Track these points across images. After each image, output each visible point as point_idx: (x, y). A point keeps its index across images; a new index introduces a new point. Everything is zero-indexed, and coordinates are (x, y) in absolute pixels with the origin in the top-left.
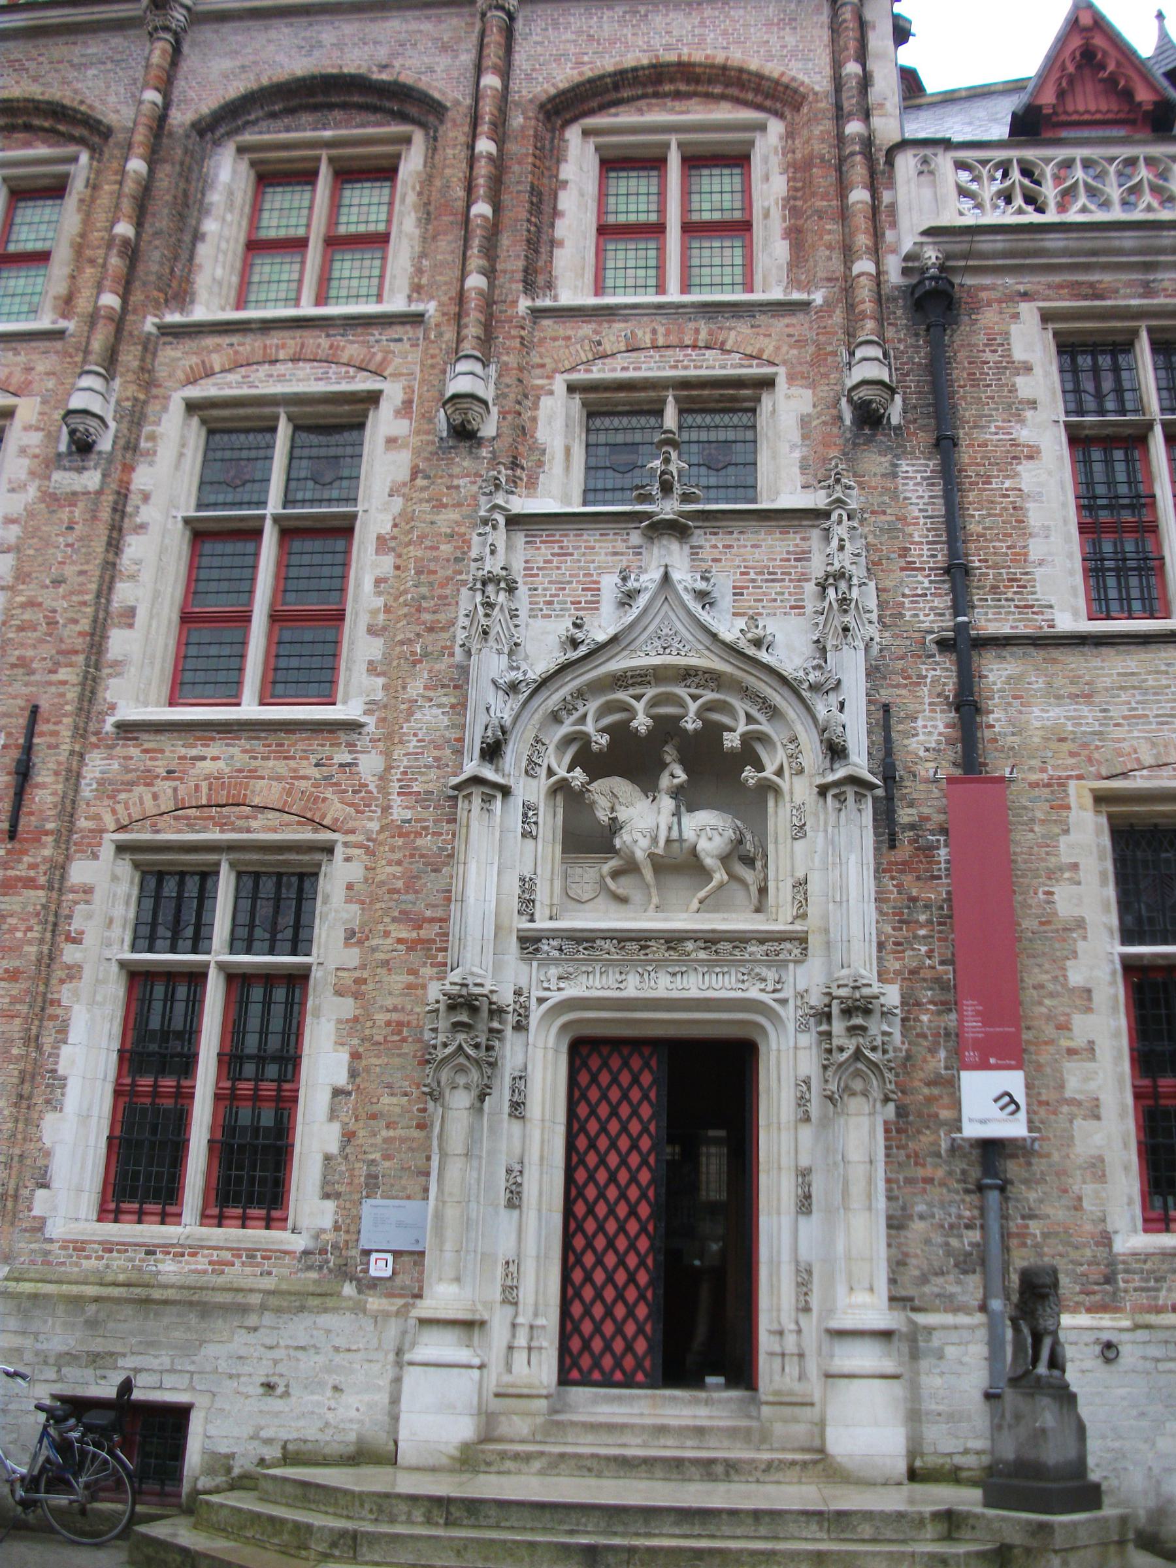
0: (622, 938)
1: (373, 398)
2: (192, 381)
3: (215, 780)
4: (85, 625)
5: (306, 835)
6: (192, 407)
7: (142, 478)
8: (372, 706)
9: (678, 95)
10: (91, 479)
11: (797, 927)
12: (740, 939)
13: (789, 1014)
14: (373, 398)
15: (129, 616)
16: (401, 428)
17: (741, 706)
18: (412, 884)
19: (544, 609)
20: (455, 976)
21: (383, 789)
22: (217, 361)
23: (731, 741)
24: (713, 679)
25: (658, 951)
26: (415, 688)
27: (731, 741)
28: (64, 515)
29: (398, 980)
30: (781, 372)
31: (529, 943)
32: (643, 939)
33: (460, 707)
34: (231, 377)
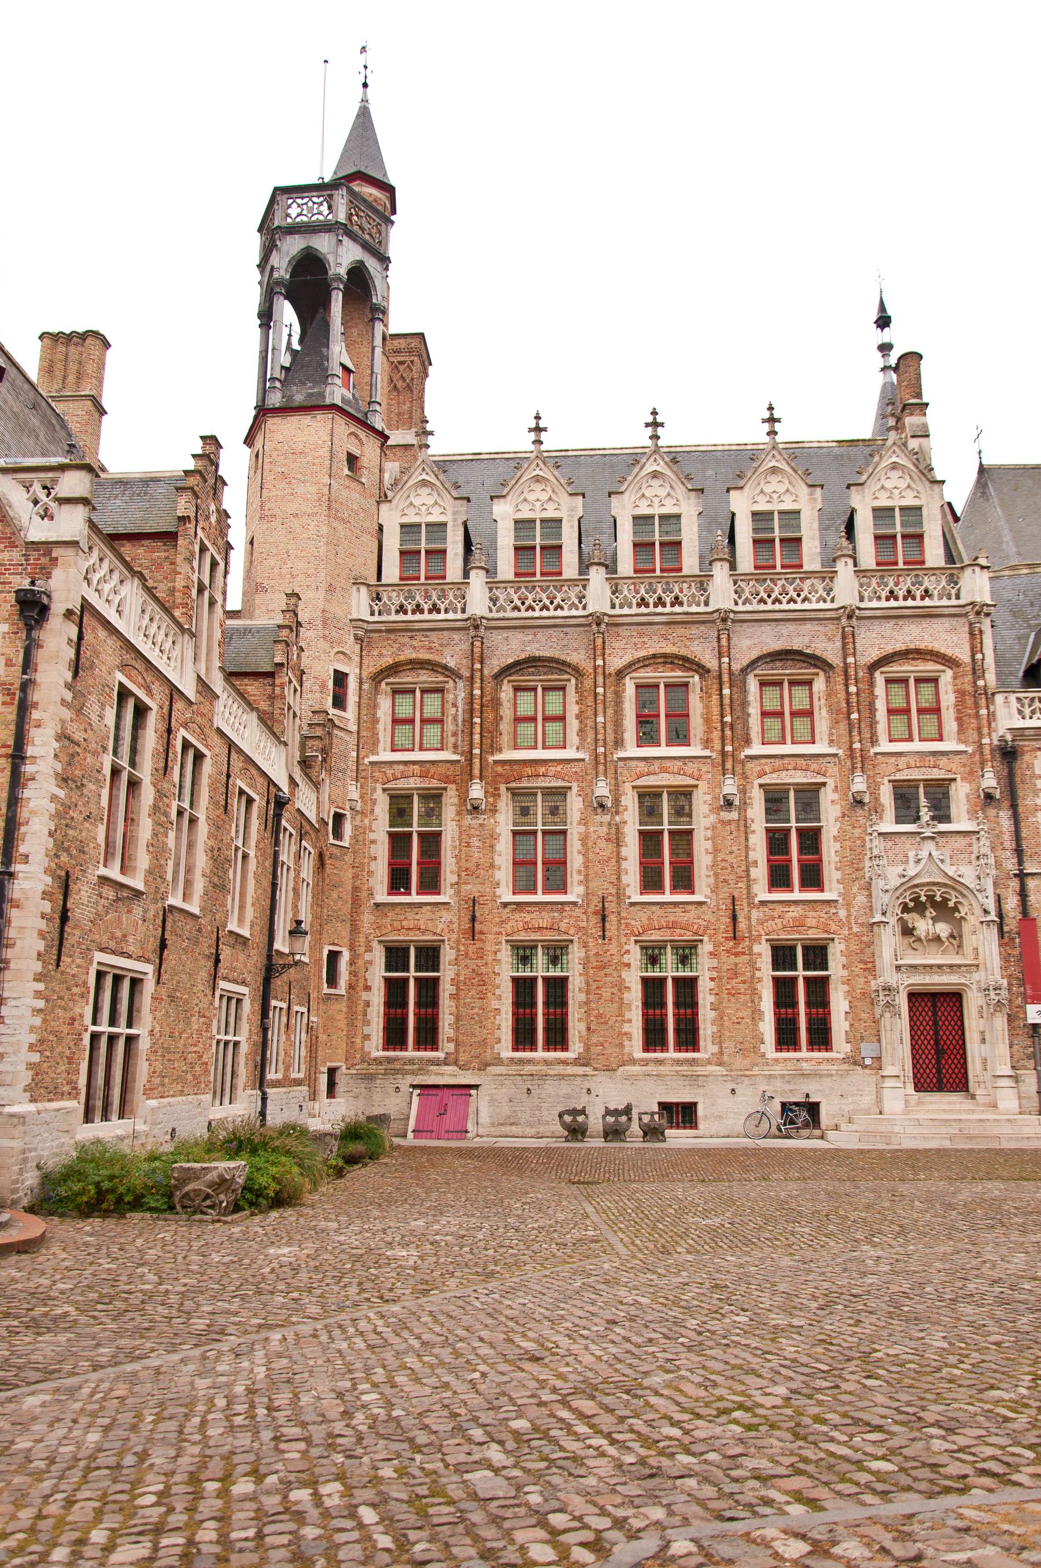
0: (925, 966)
1: (824, 784)
2: (760, 777)
3: (794, 919)
4: (744, 868)
5: (826, 936)
6: (761, 786)
7: (750, 813)
8: (840, 894)
9: (913, 659)
10: (734, 815)
11: (975, 962)
12: (959, 966)
13: (974, 987)
14: (824, 784)
15: (755, 863)
16: (835, 796)
17: (953, 893)
18: (862, 951)
19: (892, 863)
20: (881, 979)
21: (849, 922)
22: (767, 769)
23: (951, 904)
24: (945, 885)
25: (935, 969)
26: (855, 890)
27: (951, 904)
28: (728, 828)
29: (863, 980)
30: (958, 777)
31: (898, 968)
32: (931, 966)
33: (870, 896)
34: (774, 775)
